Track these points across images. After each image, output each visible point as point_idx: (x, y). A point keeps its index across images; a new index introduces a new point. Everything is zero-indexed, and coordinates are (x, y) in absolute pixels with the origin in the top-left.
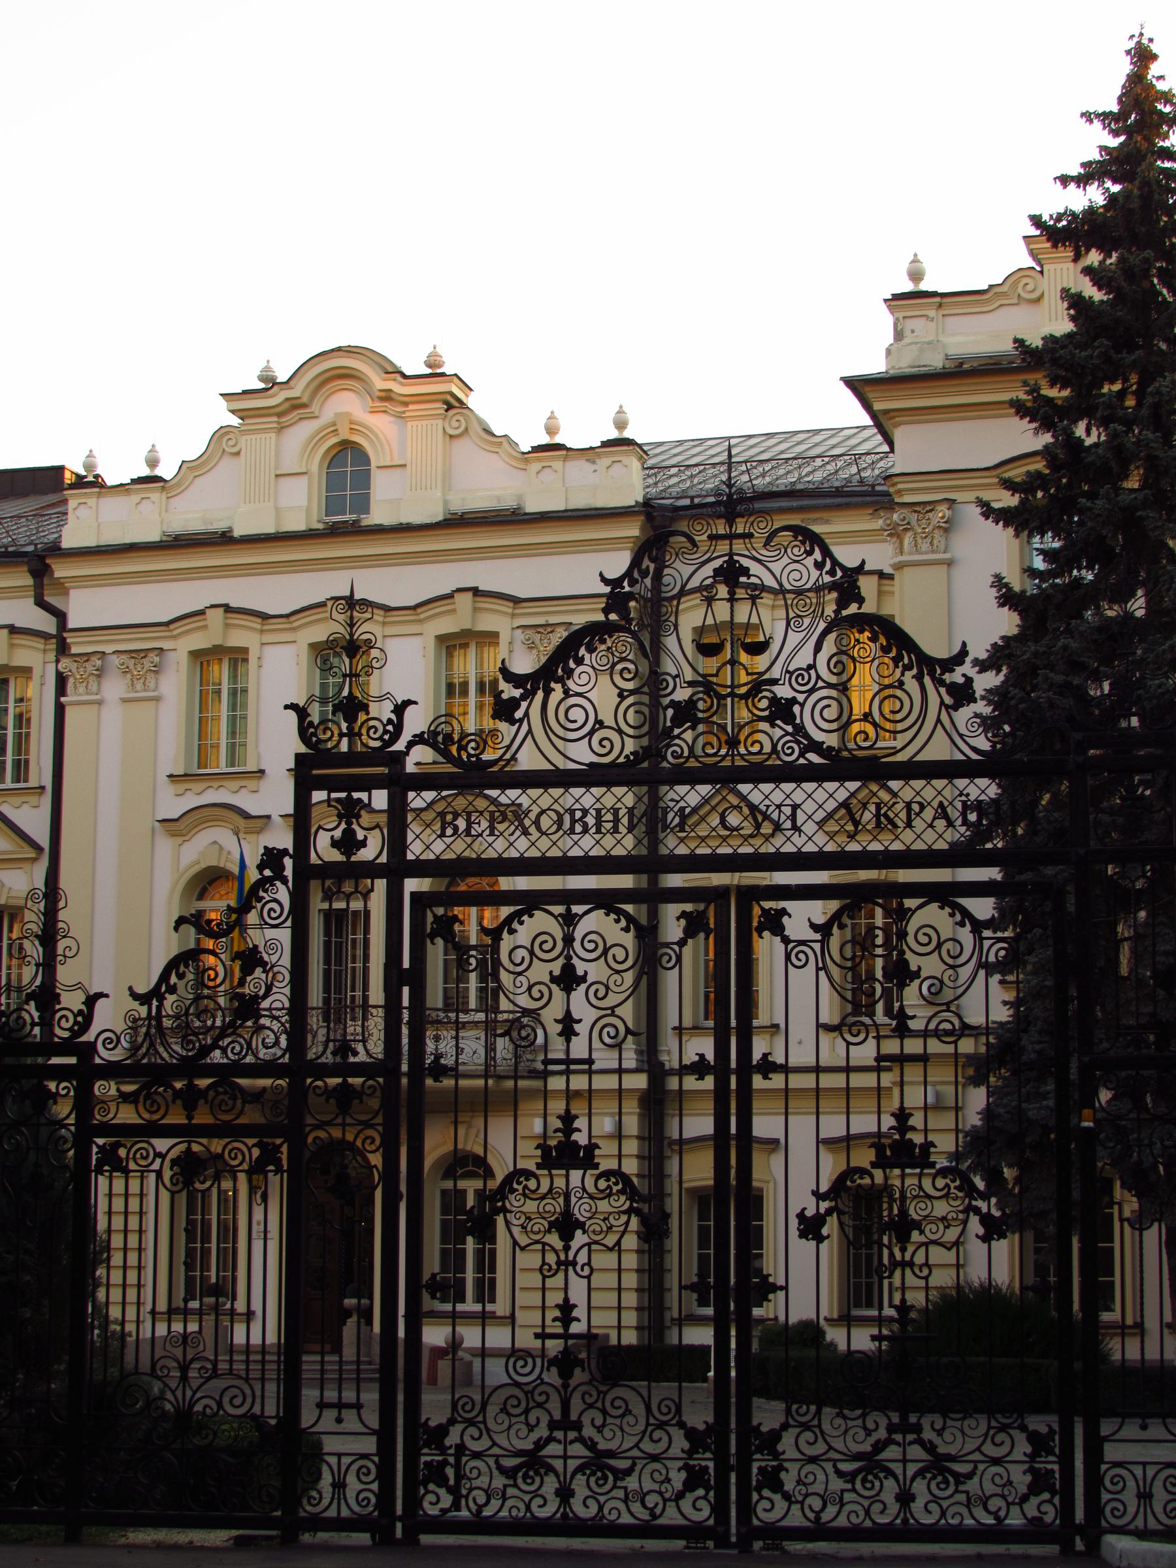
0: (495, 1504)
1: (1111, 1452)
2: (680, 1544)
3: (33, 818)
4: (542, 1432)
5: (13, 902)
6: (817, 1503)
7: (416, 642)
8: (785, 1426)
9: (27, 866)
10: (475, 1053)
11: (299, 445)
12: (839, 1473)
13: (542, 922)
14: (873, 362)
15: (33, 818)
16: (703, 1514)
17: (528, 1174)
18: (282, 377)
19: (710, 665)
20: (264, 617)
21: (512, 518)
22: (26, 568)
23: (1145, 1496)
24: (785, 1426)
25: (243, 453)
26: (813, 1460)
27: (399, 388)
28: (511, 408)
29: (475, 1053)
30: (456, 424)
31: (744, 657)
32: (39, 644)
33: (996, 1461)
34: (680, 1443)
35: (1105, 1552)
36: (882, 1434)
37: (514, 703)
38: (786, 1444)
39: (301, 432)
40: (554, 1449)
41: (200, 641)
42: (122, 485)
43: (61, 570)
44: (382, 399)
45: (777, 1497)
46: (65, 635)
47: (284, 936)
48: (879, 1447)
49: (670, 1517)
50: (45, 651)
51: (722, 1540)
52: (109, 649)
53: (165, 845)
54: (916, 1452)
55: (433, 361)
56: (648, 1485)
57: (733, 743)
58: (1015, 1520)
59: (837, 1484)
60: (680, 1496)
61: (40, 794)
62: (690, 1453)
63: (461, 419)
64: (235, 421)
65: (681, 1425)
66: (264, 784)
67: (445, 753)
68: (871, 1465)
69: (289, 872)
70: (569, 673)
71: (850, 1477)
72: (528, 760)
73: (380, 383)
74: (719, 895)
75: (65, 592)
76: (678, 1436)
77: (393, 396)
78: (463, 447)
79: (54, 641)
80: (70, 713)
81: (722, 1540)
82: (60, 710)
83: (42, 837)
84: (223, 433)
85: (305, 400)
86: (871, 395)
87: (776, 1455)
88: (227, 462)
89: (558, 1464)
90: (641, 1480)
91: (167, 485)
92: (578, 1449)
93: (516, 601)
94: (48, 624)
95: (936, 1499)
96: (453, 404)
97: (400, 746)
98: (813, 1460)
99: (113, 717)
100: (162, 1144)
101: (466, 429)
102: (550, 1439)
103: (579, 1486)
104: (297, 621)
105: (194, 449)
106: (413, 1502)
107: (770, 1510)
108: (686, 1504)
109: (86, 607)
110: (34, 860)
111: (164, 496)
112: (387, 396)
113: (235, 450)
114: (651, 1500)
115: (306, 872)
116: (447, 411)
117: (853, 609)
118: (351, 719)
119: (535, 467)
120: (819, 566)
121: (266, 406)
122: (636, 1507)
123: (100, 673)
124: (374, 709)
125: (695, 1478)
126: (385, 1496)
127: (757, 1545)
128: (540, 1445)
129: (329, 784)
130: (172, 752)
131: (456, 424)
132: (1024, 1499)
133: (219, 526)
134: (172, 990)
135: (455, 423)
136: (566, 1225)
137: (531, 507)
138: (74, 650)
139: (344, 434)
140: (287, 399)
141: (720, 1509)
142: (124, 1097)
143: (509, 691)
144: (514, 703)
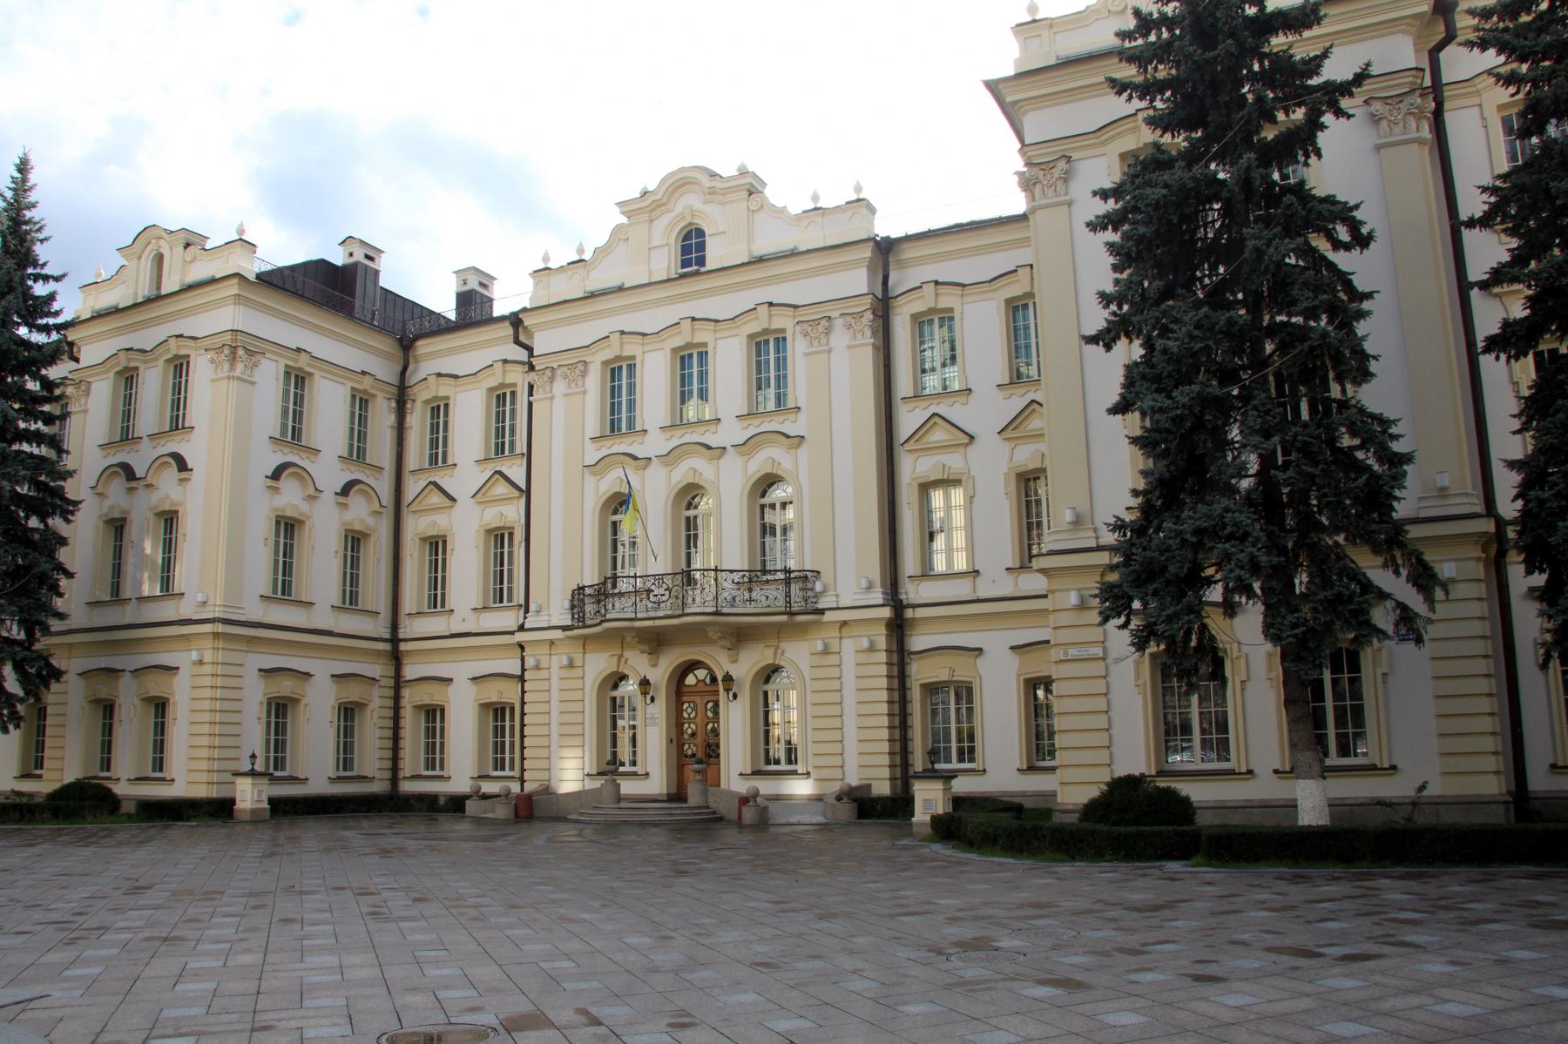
3: (517, 473)
7: (735, 340)
15: (517, 473)
21: (793, 254)
27: (718, 184)
32: (520, 368)
39: (663, 222)
43: (528, 321)
53: (590, 481)
64: (624, 220)
66: (647, 438)
73: (707, 182)
82: (530, 405)
84: (618, 229)
93: (795, 307)
94: (522, 355)
99: (559, 405)
104: (664, 335)
105: (601, 238)
112: (712, 192)
121: (642, 208)
123: (552, 380)
130: (593, 425)
133: (616, 283)
137: (802, 248)
139: (689, 220)
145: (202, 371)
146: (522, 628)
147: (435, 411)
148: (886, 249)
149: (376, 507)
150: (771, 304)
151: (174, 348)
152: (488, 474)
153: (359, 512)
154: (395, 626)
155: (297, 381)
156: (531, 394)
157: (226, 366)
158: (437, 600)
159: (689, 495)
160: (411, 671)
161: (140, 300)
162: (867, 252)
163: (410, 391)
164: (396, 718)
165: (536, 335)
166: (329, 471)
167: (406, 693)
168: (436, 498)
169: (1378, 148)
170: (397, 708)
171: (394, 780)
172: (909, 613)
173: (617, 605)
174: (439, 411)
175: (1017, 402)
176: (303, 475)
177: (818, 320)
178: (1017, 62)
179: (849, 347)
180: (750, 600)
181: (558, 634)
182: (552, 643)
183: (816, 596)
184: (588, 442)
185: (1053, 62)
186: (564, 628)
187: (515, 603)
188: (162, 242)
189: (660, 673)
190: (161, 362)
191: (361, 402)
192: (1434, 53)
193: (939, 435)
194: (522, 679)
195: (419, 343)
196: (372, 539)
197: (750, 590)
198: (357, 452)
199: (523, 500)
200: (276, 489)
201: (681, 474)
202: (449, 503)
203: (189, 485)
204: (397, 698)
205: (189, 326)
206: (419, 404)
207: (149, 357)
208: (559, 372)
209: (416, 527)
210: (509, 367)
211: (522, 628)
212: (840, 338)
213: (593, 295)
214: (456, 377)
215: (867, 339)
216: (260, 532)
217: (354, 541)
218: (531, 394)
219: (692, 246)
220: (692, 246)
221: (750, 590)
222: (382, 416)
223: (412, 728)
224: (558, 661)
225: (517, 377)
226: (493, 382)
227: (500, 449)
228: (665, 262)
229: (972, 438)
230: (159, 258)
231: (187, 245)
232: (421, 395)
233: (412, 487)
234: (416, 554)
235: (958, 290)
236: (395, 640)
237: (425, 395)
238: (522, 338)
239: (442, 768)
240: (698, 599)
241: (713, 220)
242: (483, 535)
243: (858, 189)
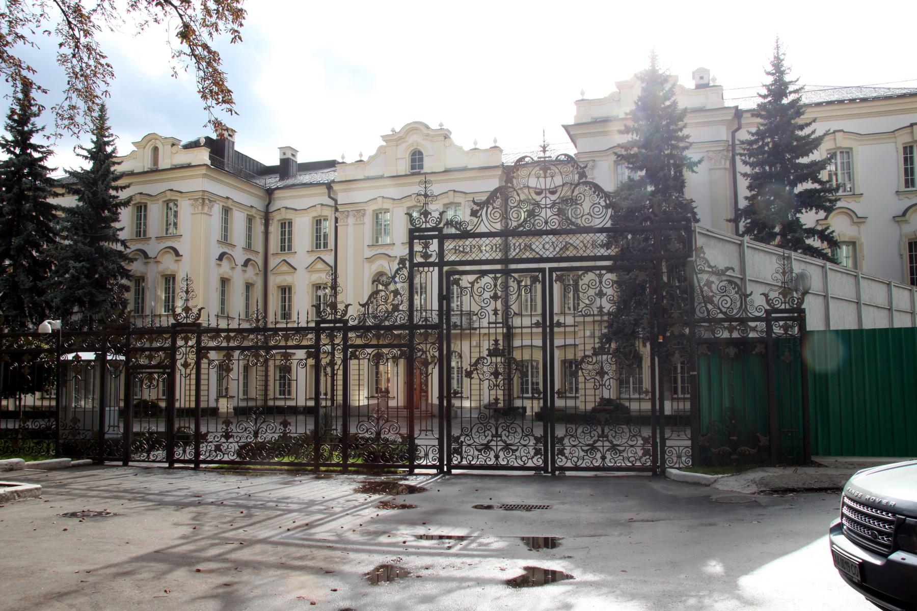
0: (475, 460)
1: (668, 443)
2: (532, 473)
4: (489, 438)
6: (576, 459)
8: (565, 436)
12: (583, 450)
13: (487, 279)
14: (571, 121)
16: (540, 463)
17: (484, 358)
18: (397, 130)
19: (538, 198)
21: (465, 169)
23: (679, 457)
24: (565, 436)
26: (574, 446)
28: (463, 139)
31: (548, 195)
32: (330, 208)
33: (632, 446)
34: (532, 442)
35: (667, 474)
36: (596, 438)
37: (477, 211)
38: (566, 441)
39: (402, 147)
40: (493, 443)
41: (375, 207)
43: (336, 187)
45: (563, 458)
47: (406, 285)
48: (595, 442)
49: (530, 464)
51: (546, 471)
53: (367, 265)
54: (607, 444)
55: (441, 125)
56: (523, 454)
57: (546, 223)
58: (638, 464)
59: (582, 454)
60: (533, 457)
62: (536, 444)
64: (384, 144)
65: (533, 435)
67: (456, 228)
68: (593, 448)
69: (407, 265)
70: (494, 202)
71: (586, 451)
72: (483, 229)
73: (426, 131)
74: (542, 270)
76: (532, 438)
81: (546, 471)
83: (332, 263)
84: (381, 147)
86: (570, 129)
87: (563, 445)
89: (495, 448)
90: (522, 452)
92: (500, 443)
94: (332, 203)
95: (613, 458)
96: (446, 137)
97: (441, 225)
98: (574, 446)
99: (351, 229)
100: (369, 350)
102: (492, 440)
103: (501, 454)
105: (373, 152)
106: (450, 460)
107: (561, 462)
108: (535, 459)
112: (428, 135)
114: (524, 459)
115: (413, 265)
117: (583, 180)
118: (426, 217)
120: (573, 166)
121: (393, 139)
122: (519, 461)
123: (348, 216)
124: (433, 214)
125: (537, 452)
126: (441, 460)
127: (557, 473)
128: (489, 442)
129: (420, 238)
130: (368, 239)
132: (641, 458)
134: (372, 303)
136: (602, 373)
137: (470, 167)
141: (545, 461)
142: (358, 336)
143: (476, 208)
144: (477, 211)
145: (185, 208)
147: (283, 225)
149: (257, 271)
150: (454, 191)
151: (169, 196)
153: (251, 272)
155: (226, 211)
156: (336, 221)
157: (200, 208)
161: (146, 170)
166: (240, 256)
168: (285, 268)
169: (710, 170)
171: (266, 400)
174: (286, 226)
176: (231, 258)
178: (575, 117)
184: (366, 247)
185: (590, 120)
188: (157, 142)
190: (160, 202)
191: (250, 220)
192: (734, 132)
195: (276, 192)
198: (249, 247)
200: (220, 265)
202: (293, 270)
203: (180, 263)
205: (177, 186)
206: (275, 221)
207: (153, 198)
208: (351, 213)
209: (275, 281)
210: (324, 208)
214: (296, 210)
216: (215, 284)
217: (249, 286)
218: (336, 221)
219: (417, 158)
220: (417, 158)
222: (259, 227)
225: (329, 213)
226: (315, 214)
227: (318, 246)
228: (403, 167)
230: (156, 149)
231: (173, 145)
232: (276, 218)
233: (273, 262)
234: (275, 294)
243: (495, 141)
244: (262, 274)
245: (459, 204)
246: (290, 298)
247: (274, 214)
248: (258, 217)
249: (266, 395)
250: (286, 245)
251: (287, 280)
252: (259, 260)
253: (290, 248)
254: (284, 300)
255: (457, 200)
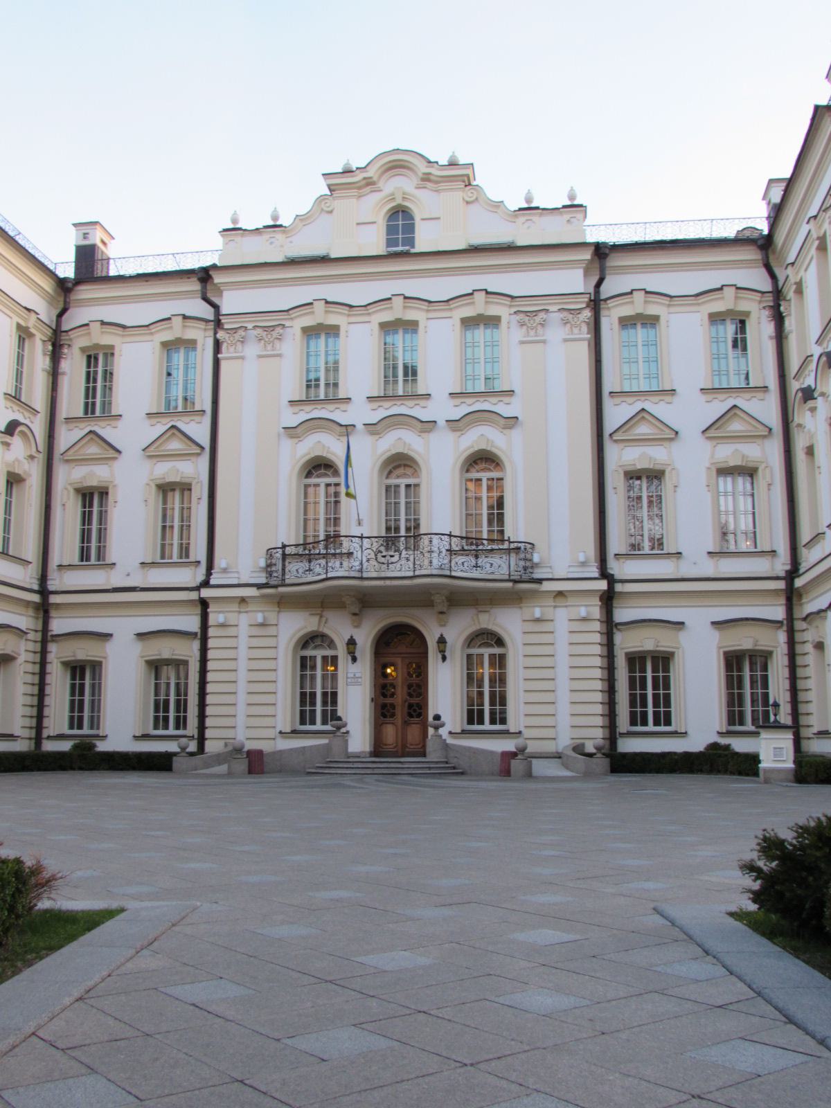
3: (199, 430)
5: (184, 480)
9: (193, 459)
10: (499, 566)
11: (373, 208)
20: (351, 306)
21: (510, 248)
22: (196, 279)
25: (335, 212)
27: (435, 172)
29: (499, 566)
30: (471, 195)
32: (202, 325)
41: (308, 321)
42: (257, 229)
43: (218, 279)
44: (423, 180)
46: (221, 317)
50: (205, 330)
52: (250, 326)
53: (287, 444)
61: (203, 415)
63: (473, 191)
73: (422, 168)
75: (220, 293)
77: (432, 177)
78: (474, 208)
79: (212, 323)
80: (224, 366)
83: (206, 443)
84: (321, 199)
85: (375, 179)
88: (325, 217)
91: (286, 229)
93: (512, 297)
94: (207, 312)
96: (468, 182)
101: (477, 199)
104: (372, 309)
105: (304, 208)
109: (231, 302)
110: (198, 455)
111: (284, 236)
112: (427, 178)
113: (330, 209)
116: (466, 186)
119: (522, 219)
123: (243, 341)
130: (293, 387)
131: (471, 195)
135: (469, 194)
137: (519, 243)
138: (226, 326)
139: (399, 201)
140: (365, 178)
146: (206, 584)
147: (91, 360)
148: (601, 252)
152: (160, 428)
154: (43, 578)
158: (92, 549)
159: (399, 463)
160: (59, 625)
162: (587, 255)
163: (64, 337)
164: (43, 674)
165: (226, 294)
167: (52, 647)
168: (94, 449)
170: (43, 663)
171: (38, 739)
172: (619, 587)
173: (345, 564)
174: (98, 362)
175: (719, 407)
177: (531, 310)
179: (566, 340)
180: (476, 566)
181: (252, 592)
182: (243, 600)
183: (532, 567)
186: (259, 586)
187: (192, 559)
189: (365, 636)
193: (643, 429)
194: (204, 637)
196: (28, 483)
197: (477, 557)
199: (204, 461)
201: (390, 443)
202: (112, 454)
204: (44, 652)
209: (66, 477)
210: (190, 323)
211: (206, 584)
212: (555, 333)
213: (292, 262)
214: (124, 327)
215: (585, 333)
221: (477, 557)
222: (39, 360)
223: (59, 684)
224: (244, 621)
228: (374, 241)
229: (677, 433)
233: (66, 437)
235: (666, 301)
236: (44, 592)
237: (84, 342)
238: (210, 296)
239: (95, 722)
240: (435, 562)
241: (424, 204)
242: (154, 488)
244: (41, 458)
245: (492, 322)
246: (102, 516)
247: (73, 335)
248: (39, 337)
249: (39, 727)
250: (97, 402)
251: (96, 474)
252: (38, 426)
253: (107, 405)
254: (86, 518)
255: (493, 311)
